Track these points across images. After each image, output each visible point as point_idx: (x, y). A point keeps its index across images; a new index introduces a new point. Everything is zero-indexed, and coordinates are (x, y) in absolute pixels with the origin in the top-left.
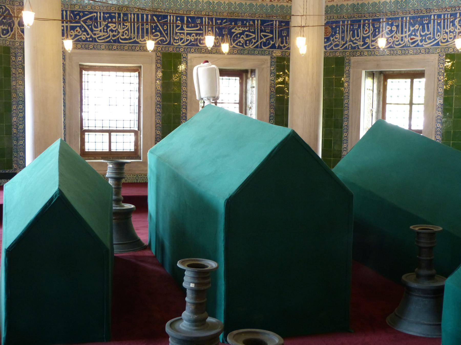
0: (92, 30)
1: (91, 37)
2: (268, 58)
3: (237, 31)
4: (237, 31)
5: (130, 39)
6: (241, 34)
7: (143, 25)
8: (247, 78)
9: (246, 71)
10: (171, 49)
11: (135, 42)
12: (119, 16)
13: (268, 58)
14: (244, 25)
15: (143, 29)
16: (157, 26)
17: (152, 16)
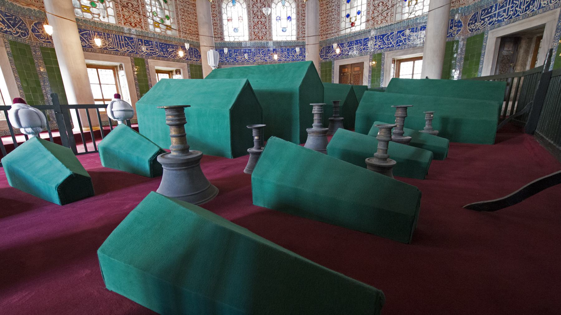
0: (87, 40)
1: (88, 45)
2: (186, 64)
3: (170, 50)
4: (170, 50)
5: (114, 48)
6: (173, 51)
7: (120, 41)
8: (172, 75)
9: (172, 72)
10: (138, 56)
11: (117, 50)
12: (104, 35)
13: (186, 64)
14: (173, 48)
15: (120, 44)
16: (128, 43)
17: (124, 37)
